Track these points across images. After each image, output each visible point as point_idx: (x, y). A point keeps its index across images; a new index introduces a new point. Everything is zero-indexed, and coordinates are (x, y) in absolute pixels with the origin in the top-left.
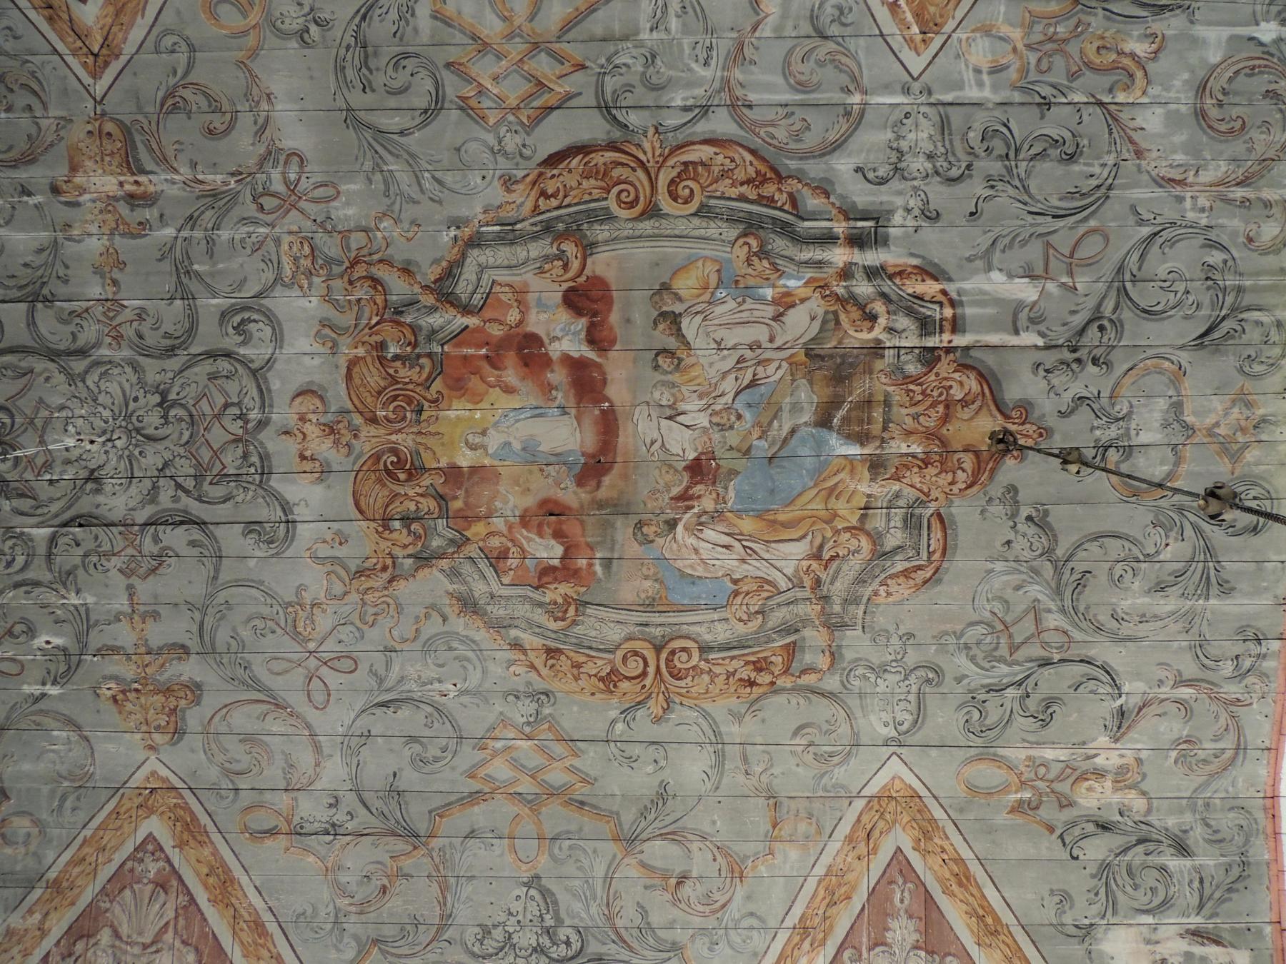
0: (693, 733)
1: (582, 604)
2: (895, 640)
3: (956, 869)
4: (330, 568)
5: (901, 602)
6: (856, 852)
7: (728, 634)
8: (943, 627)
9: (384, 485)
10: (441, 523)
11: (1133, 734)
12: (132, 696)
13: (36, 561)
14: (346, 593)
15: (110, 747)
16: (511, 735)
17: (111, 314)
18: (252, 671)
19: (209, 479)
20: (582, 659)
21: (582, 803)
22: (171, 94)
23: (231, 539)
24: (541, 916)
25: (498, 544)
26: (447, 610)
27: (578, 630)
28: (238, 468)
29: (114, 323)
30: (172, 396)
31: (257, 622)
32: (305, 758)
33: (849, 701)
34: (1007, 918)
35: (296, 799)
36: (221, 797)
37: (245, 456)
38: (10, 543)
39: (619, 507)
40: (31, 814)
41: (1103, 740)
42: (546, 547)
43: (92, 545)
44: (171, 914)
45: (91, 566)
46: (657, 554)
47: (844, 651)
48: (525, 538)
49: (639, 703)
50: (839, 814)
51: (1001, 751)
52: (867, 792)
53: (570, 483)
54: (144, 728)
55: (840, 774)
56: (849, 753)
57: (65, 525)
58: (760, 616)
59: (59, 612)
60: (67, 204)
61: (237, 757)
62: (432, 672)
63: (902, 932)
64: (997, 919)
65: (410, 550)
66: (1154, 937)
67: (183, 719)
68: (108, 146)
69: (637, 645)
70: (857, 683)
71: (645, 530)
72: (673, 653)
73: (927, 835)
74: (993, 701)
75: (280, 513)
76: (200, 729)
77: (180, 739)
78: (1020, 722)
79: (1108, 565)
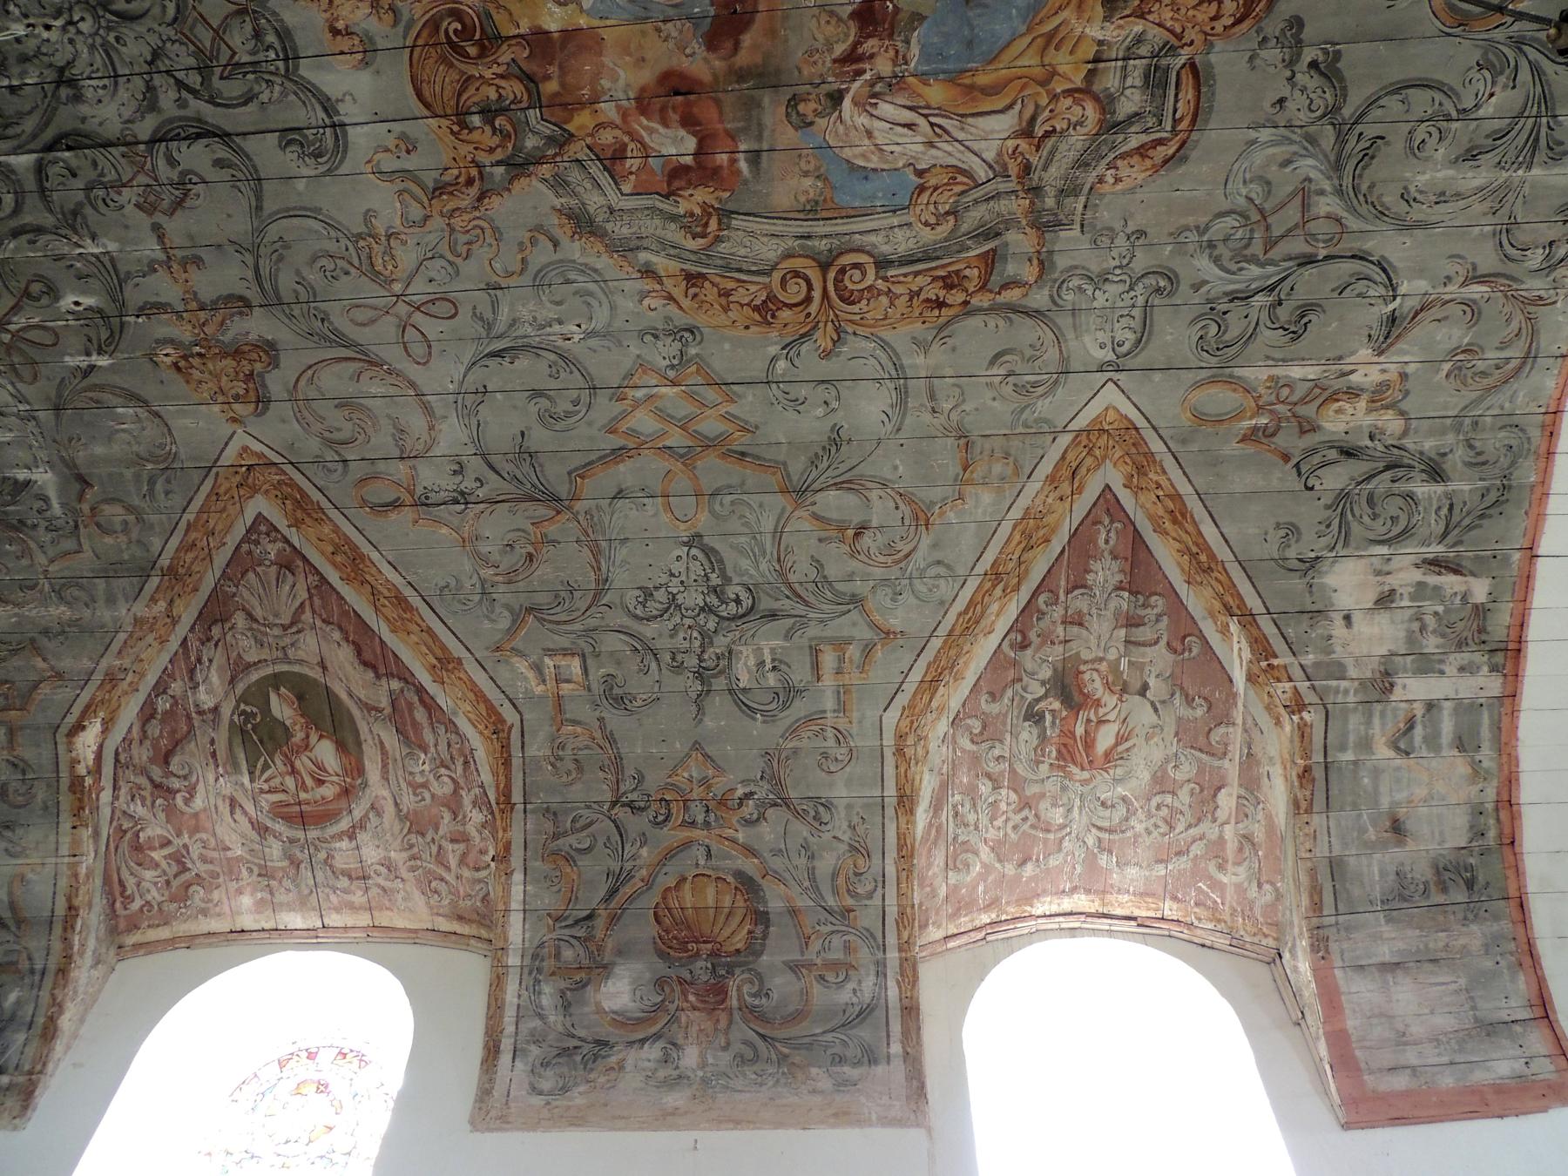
0: (870, 368)
1: (725, 214)
2: (1121, 241)
3: (1171, 505)
4: (402, 186)
5: (1132, 191)
6: (1057, 493)
7: (911, 244)
8: (1183, 221)
9: (451, 65)
10: (533, 114)
11: (1400, 345)
12: (196, 361)
13: (28, 201)
14: (427, 218)
15: (187, 422)
16: (654, 382)
18: (331, 323)
19: (218, 71)
20: (731, 285)
21: (743, 454)
23: (265, 151)
24: (706, 575)
25: (611, 140)
26: (557, 233)
27: (723, 248)
28: (253, 53)
31: (323, 262)
32: (417, 423)
33: (1059, 321)
34: (1223, 553)
35: (413, 468)
36: (329, 470)
37: (258, 34)
39: (766, 77)
40: (120, 501)
41: (1365, 353)
42: (677, 141)
43: (93, 175)
44: (305, 595)
45: (100, 202)
46: (819, 141)
47: (1056, 257)
48: (645, 128)
49: (802, 336)
50: (1041, 452)
51: (1238, 372)
52: (1074, 426)
53: (697, 46)
54: (221, 399)
55: (1043, 407)
56: (1056, 381)
57: (49, 148)
58: (951, 218)
59: (78, 265)
61: (336, 424)
62: (550, 312)
63: (1105, 573)
64: (1212, 556)
65: (499, 155)
66: (1386, 568)
67: (264, 386)
69: (797, 263)
70: (1069, 297)
71: (801, 107)
72: (843, 271)
73: (1141, 471)
74: (1237, 310)
75: (321, 114)
76: (286, 396)
77: (266, 409)
78: (1267, 335)
79: (1406, 127)
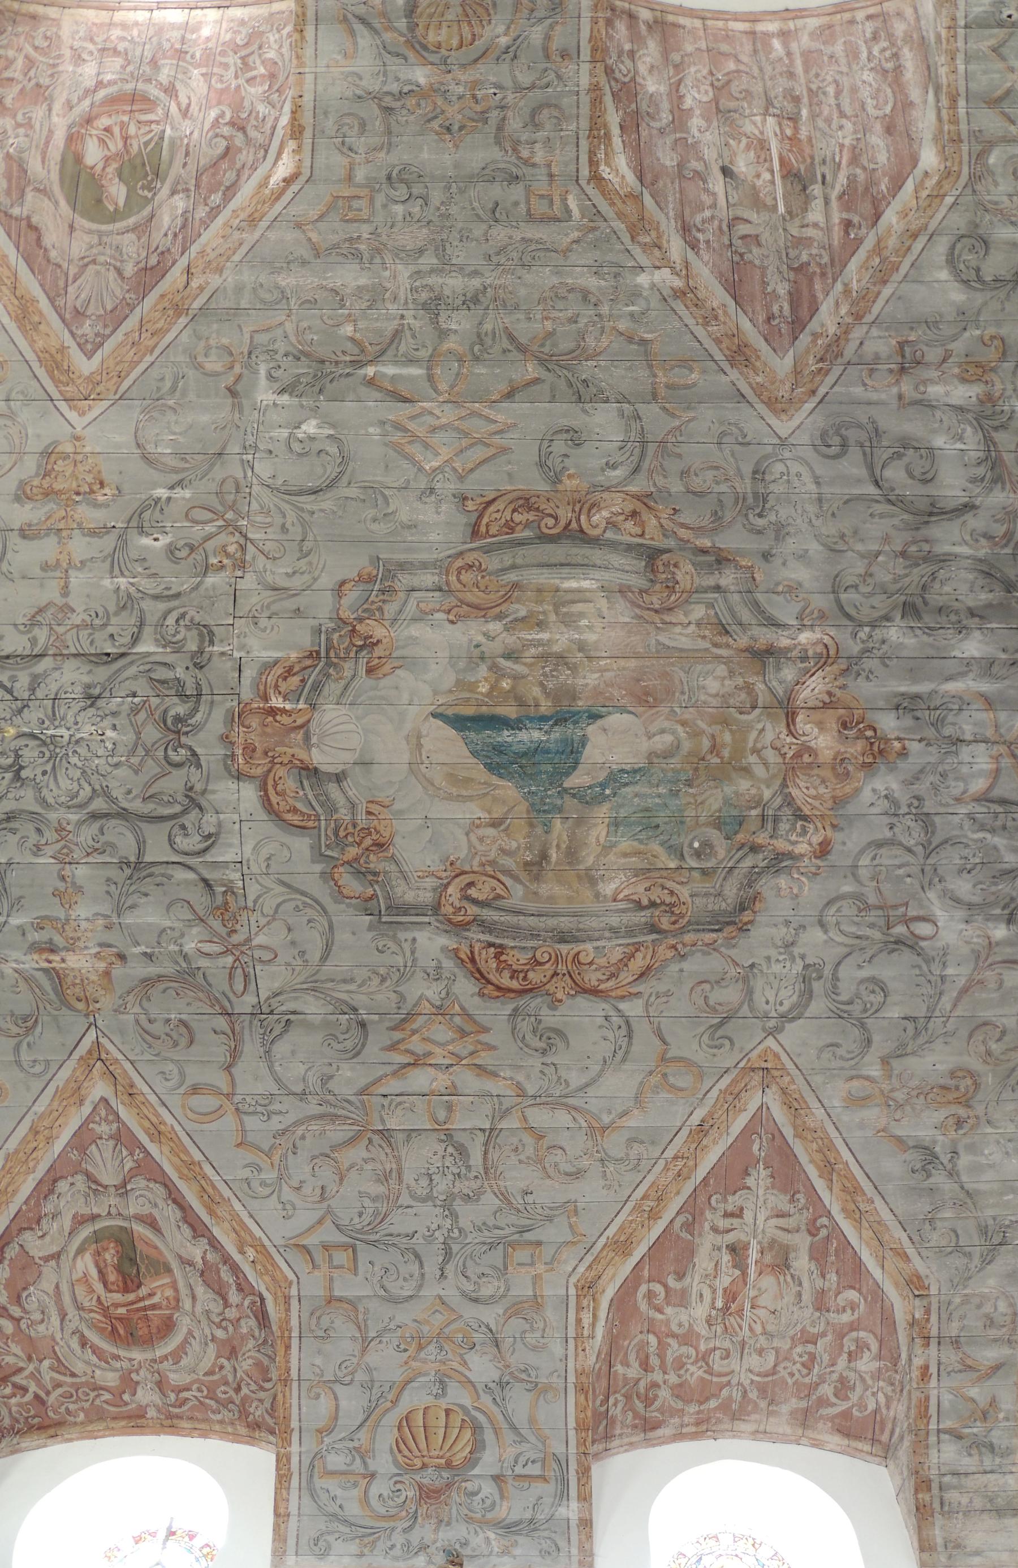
17: (65, 851)
22: (29, 1030)
29: (63, 843)
30: (9, 776)
38: (179, 637)
54: (79, 457)
59: (140, 570)
60: (110, 946)
67: (39, 466)
68: (77, 990)
